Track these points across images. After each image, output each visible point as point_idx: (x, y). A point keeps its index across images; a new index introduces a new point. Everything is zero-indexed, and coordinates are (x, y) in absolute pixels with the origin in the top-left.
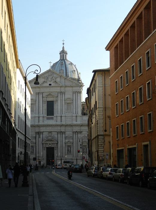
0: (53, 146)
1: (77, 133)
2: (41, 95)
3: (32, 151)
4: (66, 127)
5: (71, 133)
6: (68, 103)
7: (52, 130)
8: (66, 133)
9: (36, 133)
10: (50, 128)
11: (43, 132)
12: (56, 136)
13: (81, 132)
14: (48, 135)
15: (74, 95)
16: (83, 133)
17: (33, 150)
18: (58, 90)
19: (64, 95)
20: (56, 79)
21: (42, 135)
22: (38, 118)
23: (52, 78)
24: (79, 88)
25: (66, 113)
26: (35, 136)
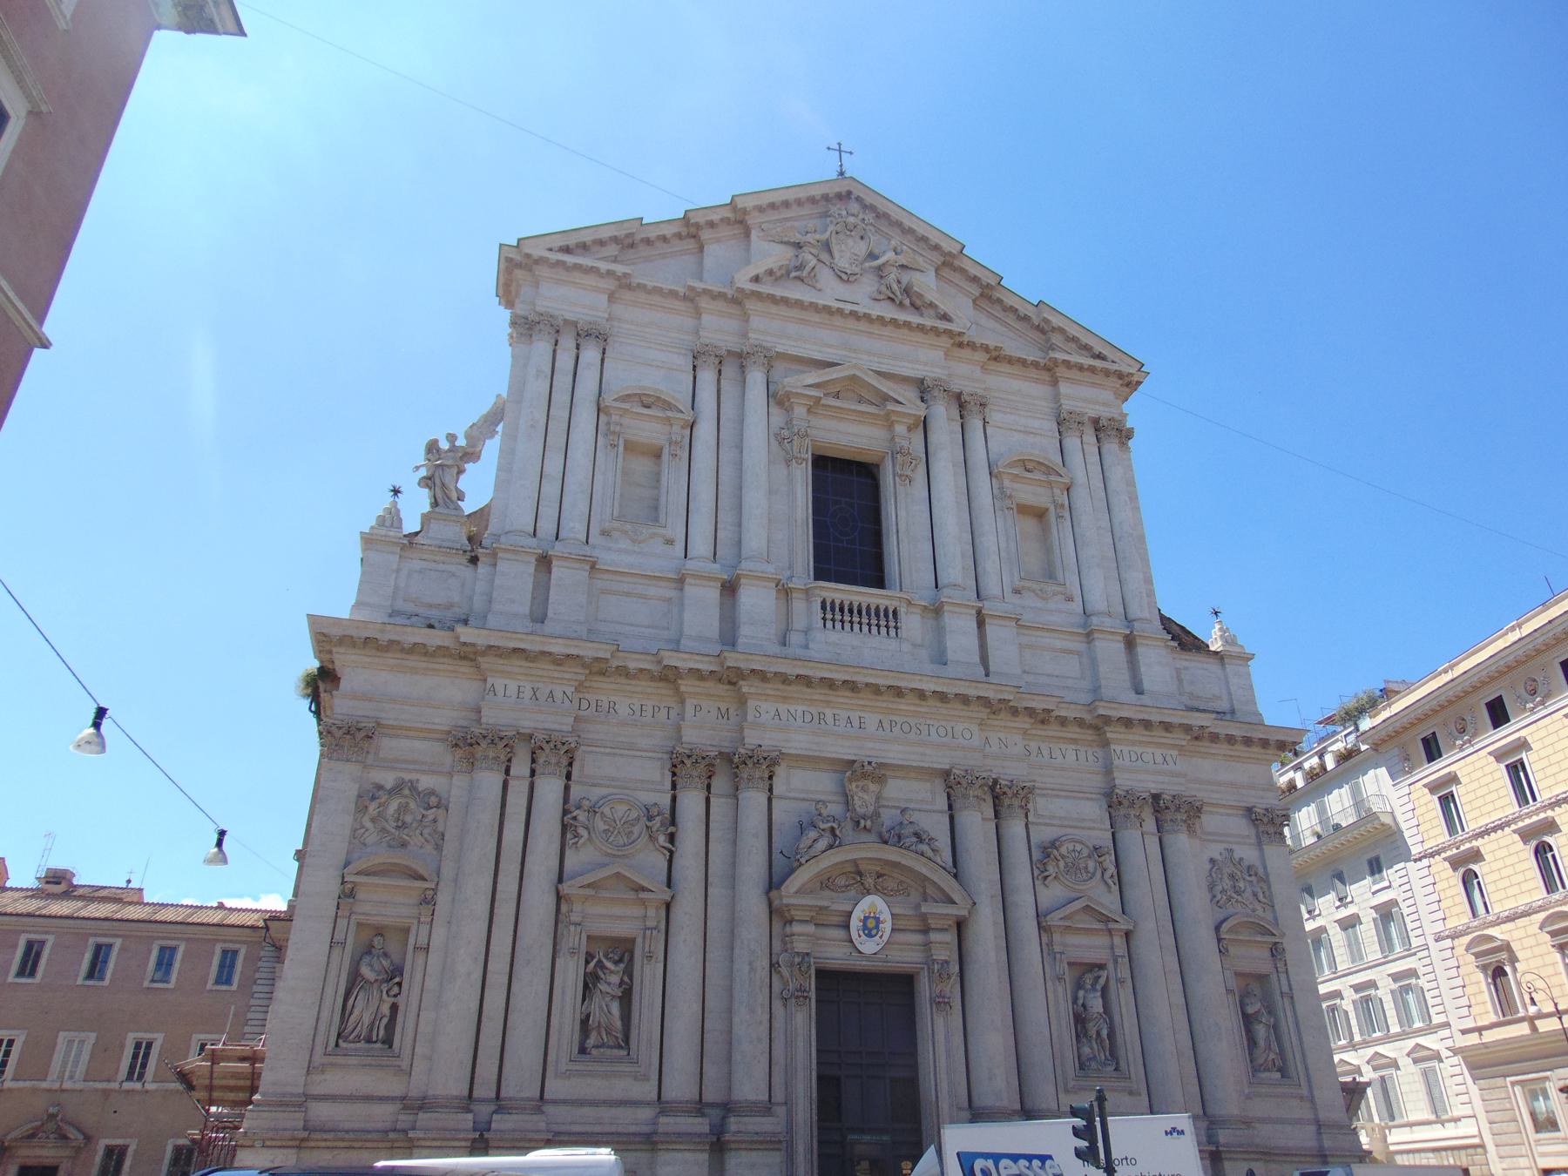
0: (905, 957)
1: (1150, 825)
2: (756, 378)
3: (615, 1008)
4: (1033, 745)
5: (1094, 810)
6: (1024, 510)
7: (894, 753)
8: (1042, 806)
9: (678, 765)
10: (871, 720)
11: (766, 764)
12: (936, 826)
13: (1194, 810)
14: (835, 809)
15: (1072, 443)
16: (1209, 821)
17: (626, 998)
18: (926, 360)
19: (975, 424)
20: (902, 266)
21: (762, 798)
22: (712, 594)
23: (872, 256)
24: (1107, 395)
25: (1017, 591)
26: (666, 800)
